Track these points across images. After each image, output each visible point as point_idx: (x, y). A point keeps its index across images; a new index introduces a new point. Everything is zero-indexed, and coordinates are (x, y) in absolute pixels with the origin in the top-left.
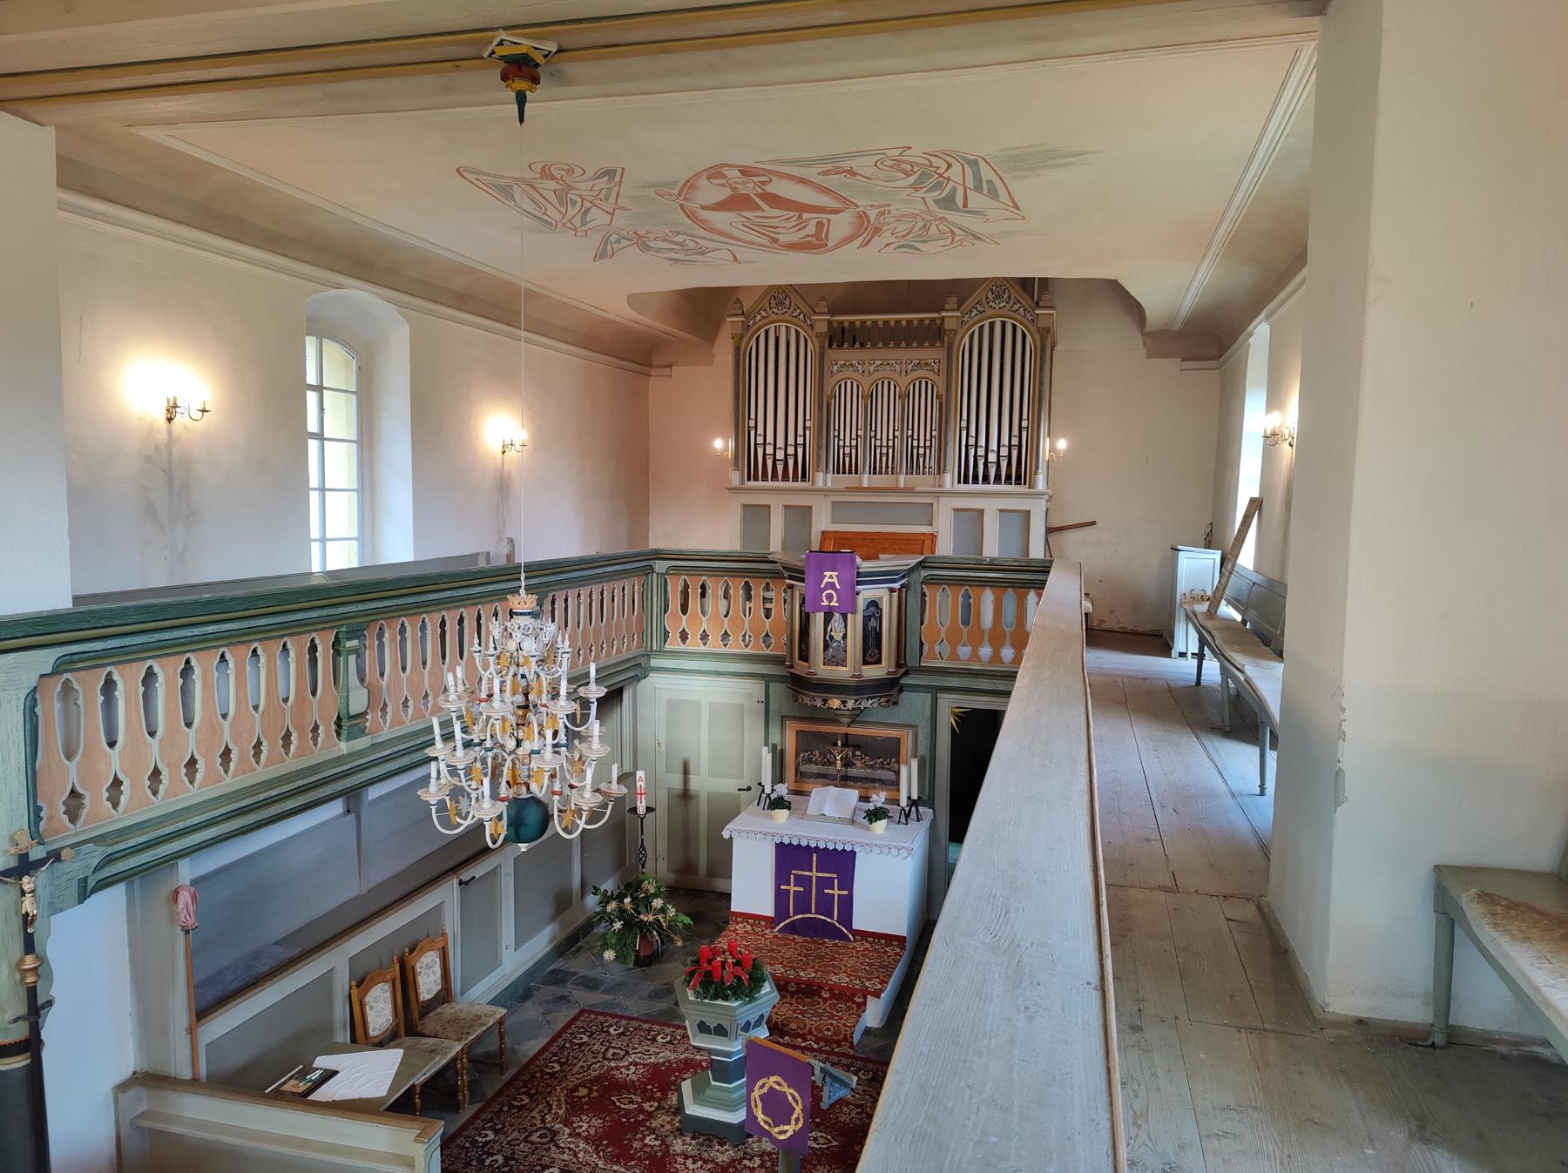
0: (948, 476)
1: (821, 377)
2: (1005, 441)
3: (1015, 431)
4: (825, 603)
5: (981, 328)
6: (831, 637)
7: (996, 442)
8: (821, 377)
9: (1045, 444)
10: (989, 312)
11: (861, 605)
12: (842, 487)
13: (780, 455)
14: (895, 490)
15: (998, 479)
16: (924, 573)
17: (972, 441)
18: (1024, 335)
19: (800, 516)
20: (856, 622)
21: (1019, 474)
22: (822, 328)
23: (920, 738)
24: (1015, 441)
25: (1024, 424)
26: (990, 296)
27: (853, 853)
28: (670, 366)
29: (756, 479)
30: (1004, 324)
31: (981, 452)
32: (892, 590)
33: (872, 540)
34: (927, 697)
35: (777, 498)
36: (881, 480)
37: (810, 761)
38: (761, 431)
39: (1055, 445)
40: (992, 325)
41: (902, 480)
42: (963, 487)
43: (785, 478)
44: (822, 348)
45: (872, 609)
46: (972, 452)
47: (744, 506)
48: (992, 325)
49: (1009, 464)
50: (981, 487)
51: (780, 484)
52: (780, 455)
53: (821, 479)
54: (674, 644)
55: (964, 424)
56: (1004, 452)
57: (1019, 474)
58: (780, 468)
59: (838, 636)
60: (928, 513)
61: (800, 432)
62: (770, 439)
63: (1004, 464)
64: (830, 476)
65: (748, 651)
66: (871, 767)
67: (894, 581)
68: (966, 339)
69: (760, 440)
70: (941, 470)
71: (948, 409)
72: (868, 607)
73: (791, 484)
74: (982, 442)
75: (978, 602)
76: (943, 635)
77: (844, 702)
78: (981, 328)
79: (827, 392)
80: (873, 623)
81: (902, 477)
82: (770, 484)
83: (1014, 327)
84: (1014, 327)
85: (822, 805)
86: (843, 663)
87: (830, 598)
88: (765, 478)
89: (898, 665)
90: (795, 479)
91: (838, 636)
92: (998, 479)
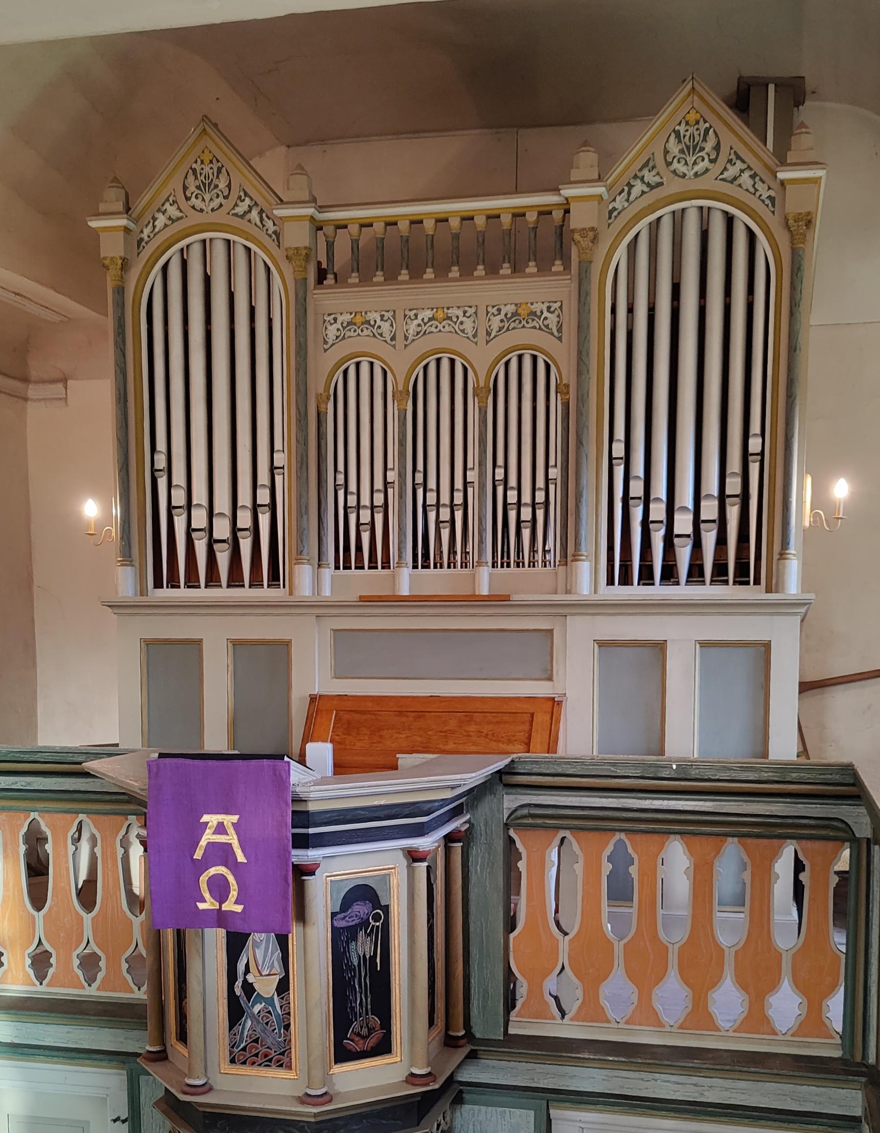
0: (584, 568)
1: (302, 351)
2: (711, 485)
7: (691, 492)
8: (302, 351)
10: (673, 187)
11: (322, 897)
12: (352, 596)
14: (472, 600)
16: (511, 801)
17: (636, 488)
19: (264, 661)
20: (314, 943)
21: (743, 561)
25: (755, 445)
26: (674, 147)
28: (64, 380)
29: (174, 583)
30: (704, 214)
32: (414, 856)
33: (420, 715)
35: (217, 624)
36: (436, 581)
38: (179, 477)
39: (822, 493)
40: (678, 218)
41: (485, 580)
42: (619, 592)
43: (235, 580)
45: (361, 909)
48: (678, 218)
50: (658, 591)
51: (223, 593)
53: (306, 580)
55: (619, 450)
56: (709, 510)
57: (743, 561)
60: (541, 652)
61: (263, 478)
62: (200, 495)
63: (709, 539)
64: (328, 573)
65: (92, 991)
67: (420, 831)
68: (621, 254)
69: (179, 497)
70: (568, 555)
71: (579, 413)
72: (347, 902)
73: (246, 593)
74: (660, 489)
75: (650, 873)
76: (563, 958)
80: (363, 946)
82: (203, 593)
83: (730, 220)
86: (280, 1058)
87: (219, 889)
88: (192, 581)
89: (450, 1042)
90: (255, 582)
92: (696, 572)
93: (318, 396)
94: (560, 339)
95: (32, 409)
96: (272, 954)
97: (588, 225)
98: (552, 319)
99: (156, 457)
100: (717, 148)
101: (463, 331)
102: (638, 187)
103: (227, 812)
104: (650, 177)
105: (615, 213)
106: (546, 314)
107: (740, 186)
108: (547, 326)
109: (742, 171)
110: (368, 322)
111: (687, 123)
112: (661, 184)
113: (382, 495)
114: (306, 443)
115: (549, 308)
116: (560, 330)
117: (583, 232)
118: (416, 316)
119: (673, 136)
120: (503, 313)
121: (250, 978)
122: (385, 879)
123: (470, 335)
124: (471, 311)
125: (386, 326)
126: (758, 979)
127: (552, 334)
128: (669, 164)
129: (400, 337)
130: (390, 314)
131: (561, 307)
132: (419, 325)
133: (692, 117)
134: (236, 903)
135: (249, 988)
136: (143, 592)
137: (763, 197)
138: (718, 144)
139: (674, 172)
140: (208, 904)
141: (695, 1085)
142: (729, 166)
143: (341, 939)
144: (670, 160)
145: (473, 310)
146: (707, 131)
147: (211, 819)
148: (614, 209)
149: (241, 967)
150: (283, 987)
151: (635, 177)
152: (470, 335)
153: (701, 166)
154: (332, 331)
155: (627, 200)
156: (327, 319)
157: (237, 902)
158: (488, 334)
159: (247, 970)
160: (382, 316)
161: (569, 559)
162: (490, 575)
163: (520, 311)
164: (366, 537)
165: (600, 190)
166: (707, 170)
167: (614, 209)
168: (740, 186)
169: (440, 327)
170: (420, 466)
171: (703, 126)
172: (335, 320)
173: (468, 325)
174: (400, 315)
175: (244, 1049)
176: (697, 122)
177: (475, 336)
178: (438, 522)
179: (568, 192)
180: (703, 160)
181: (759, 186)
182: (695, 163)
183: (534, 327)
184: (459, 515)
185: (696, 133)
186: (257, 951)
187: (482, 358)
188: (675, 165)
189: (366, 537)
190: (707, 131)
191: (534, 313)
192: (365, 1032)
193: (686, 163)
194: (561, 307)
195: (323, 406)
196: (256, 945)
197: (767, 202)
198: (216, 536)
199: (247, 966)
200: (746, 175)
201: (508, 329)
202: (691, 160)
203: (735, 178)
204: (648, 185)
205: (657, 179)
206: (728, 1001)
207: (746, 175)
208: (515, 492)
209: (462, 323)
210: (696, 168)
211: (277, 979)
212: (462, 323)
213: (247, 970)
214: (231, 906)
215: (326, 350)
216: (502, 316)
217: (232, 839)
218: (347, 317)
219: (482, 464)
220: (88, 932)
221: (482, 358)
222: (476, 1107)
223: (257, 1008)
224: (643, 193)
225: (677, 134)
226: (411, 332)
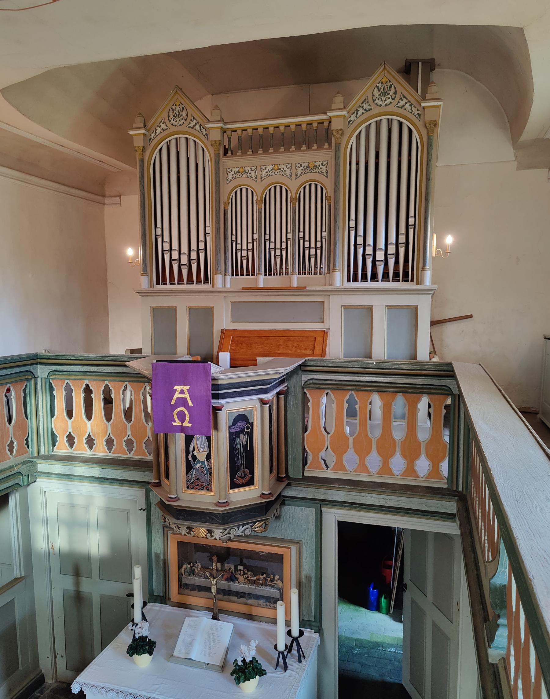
0: (337, 276)
1: (217, 183)
3: (402, 230)
5: (368, 128)
7: (383, 242)
8: (217, 183)
9: (432, 241)
11: (224, 420)
12: (239, 287)
13: (184, 260)
14: (290, 289)
16: (305, 377)
17: (360, 241)
18: (410, 131)
19: (202, 315)
22: (216, 136)
23: (304, 555)
24: (402, 239)
26: (376, 93)
28: (120, 196)
29: (164, 283)
30: (390, 122)
31: (369, 250)
32: (263, 402)
34: (310, 512)
36: (274, 281)
37: (192, 572)
38: (166, 238)
40: (378, 124)
41: (295, 280)
42: (353, 285)
43: (190, 281)
44: (217, 156)
45: (241, 424)
46: (360, 251)
47: (190, 308)
48: (378, 124)
49: (397, 262)
50: (370, 284)
53: (221, 281)
54: (62, 449)
55: (352, 224)
58: (185, 272)
60: (319, 310)
61: (202, 238)
62: (175, 245)
64: (229, 278)
65: (131, 456)
66: (254, 582)
67: (266, 391)
68: (353, 139)
69: (166, 247)
70: (331, 270)
71: (335, 209)
72: (235, 422)
76: (327, 443)
78: (368, 128)
79: (224, 198)
80: (242, 440)
81: (295, 277)
82: (176, 287)
83: (401, 124)
84: (401, 124)
85: (191, 644)
86: (208, 487)
87: (182, 416)
88: (172, 282)
90: (198, 282)
93: (224, 203)
94: (327, 177)
95: (107, 208)
96: (204, 443)
97: (339, 128)
98: (324, 168)
99: (157, 230)
100: (395, 93)
101: (286, 174)
102: (361, 111)
103: (185, 385)
104: (366, 106)
105: (351, 122)
106: (321, 166)
107: (405, 109)
108: (322, 172)
109: (406, 103)
110: (245, 171)
111: (382, 83)
112: (371, 109)
113: (251, 245)
114: (219, 223)
115: (322, 164)
116: (327, 173)
117: (337, 131)
118: (266, 168)
119: (376, 88)
120: (303, 166)
121: (195, 453)
122: (251, 412)
123: (289, 176)
124: (289, 166)
125: (253, 173)
126: (411, 455)
127: (324, 175)
128: (374, 101)
129: (259, 177)
130: (254, 168)
131: (327, 163)
132: (267, 172)
133: (384, 80)
134: (189, 423)
135: (194, 457)
136: (152, 286)
137: (415, 114)
138: (396, 91)
139: (377, 104)
140: (177, 423)
141: (384, 499)
142: (400, 101)
143: (233, 437)
144: (374, 99)
145: (290, 165)
146: (391, 86)
147: (178, 388)
148: (351, 121)
149: (191, 448)
150: (209, 457)
151: (360, 107)
152: (289, 176)
153: (388, 101)
154: (230, 175)
155: (356, 117)
156: (228, 170)
157: (189, 423)
158: (296, 175)
159: (194, 450)
160: (251, 169)
161: (331, 271)
162: (297, 278)
163: (310, 165)
164: (245, 262)
165: (344, 113)
166: (391, 103)
167: (351, 121)
168: (405, 109)
169: (276, 173)
170: (268, 232)
171: (389, 84)
172: (232, 170)
173: (288, 172)
174: (259, 168)
175: (192, 483)
176: (387, 82)
177: (291, 176)
178: (275, 256)
179: (330, 114)
180: (389, 98)
181: (414, 109)
182: (386, 100)
183: (316, 172)
184: (284, 253)
185: (386, 87)
186: (198, 442)
187: (294, 185)
188: (377, 101)
189: (245, 262)
190: (391, 86)
191: (316, 166)
192: (243, 476)
193: (382, 100)
194: (327, 163)
195: (226, 207)
196: (197, 439)
197: (417, 116)
198: (182, 262)
199: (194, 448)
200: (408, 104)
201: (305, 173)
202: (384, 98)
203: (403, 106)
204: (365, 110)
205: (369, 107)
206: (398, 463)
207: (408, 104)
208: (308, 243)
209: (285, 171)
210: (386, 102)
211: (206, 453)
212: (285, 171)
213: (194, 450)
214: (186, 424)
215: (227, 184)
216: (302, 168)
217: (187, 396)
218: (237, 169)
219: (294, 231)
220: (129, 431)
221: (294, 185)
222: (290, 507)
223: (198, 466)
224: (363, 113)
225: (378, 87)
226: (264, 175)
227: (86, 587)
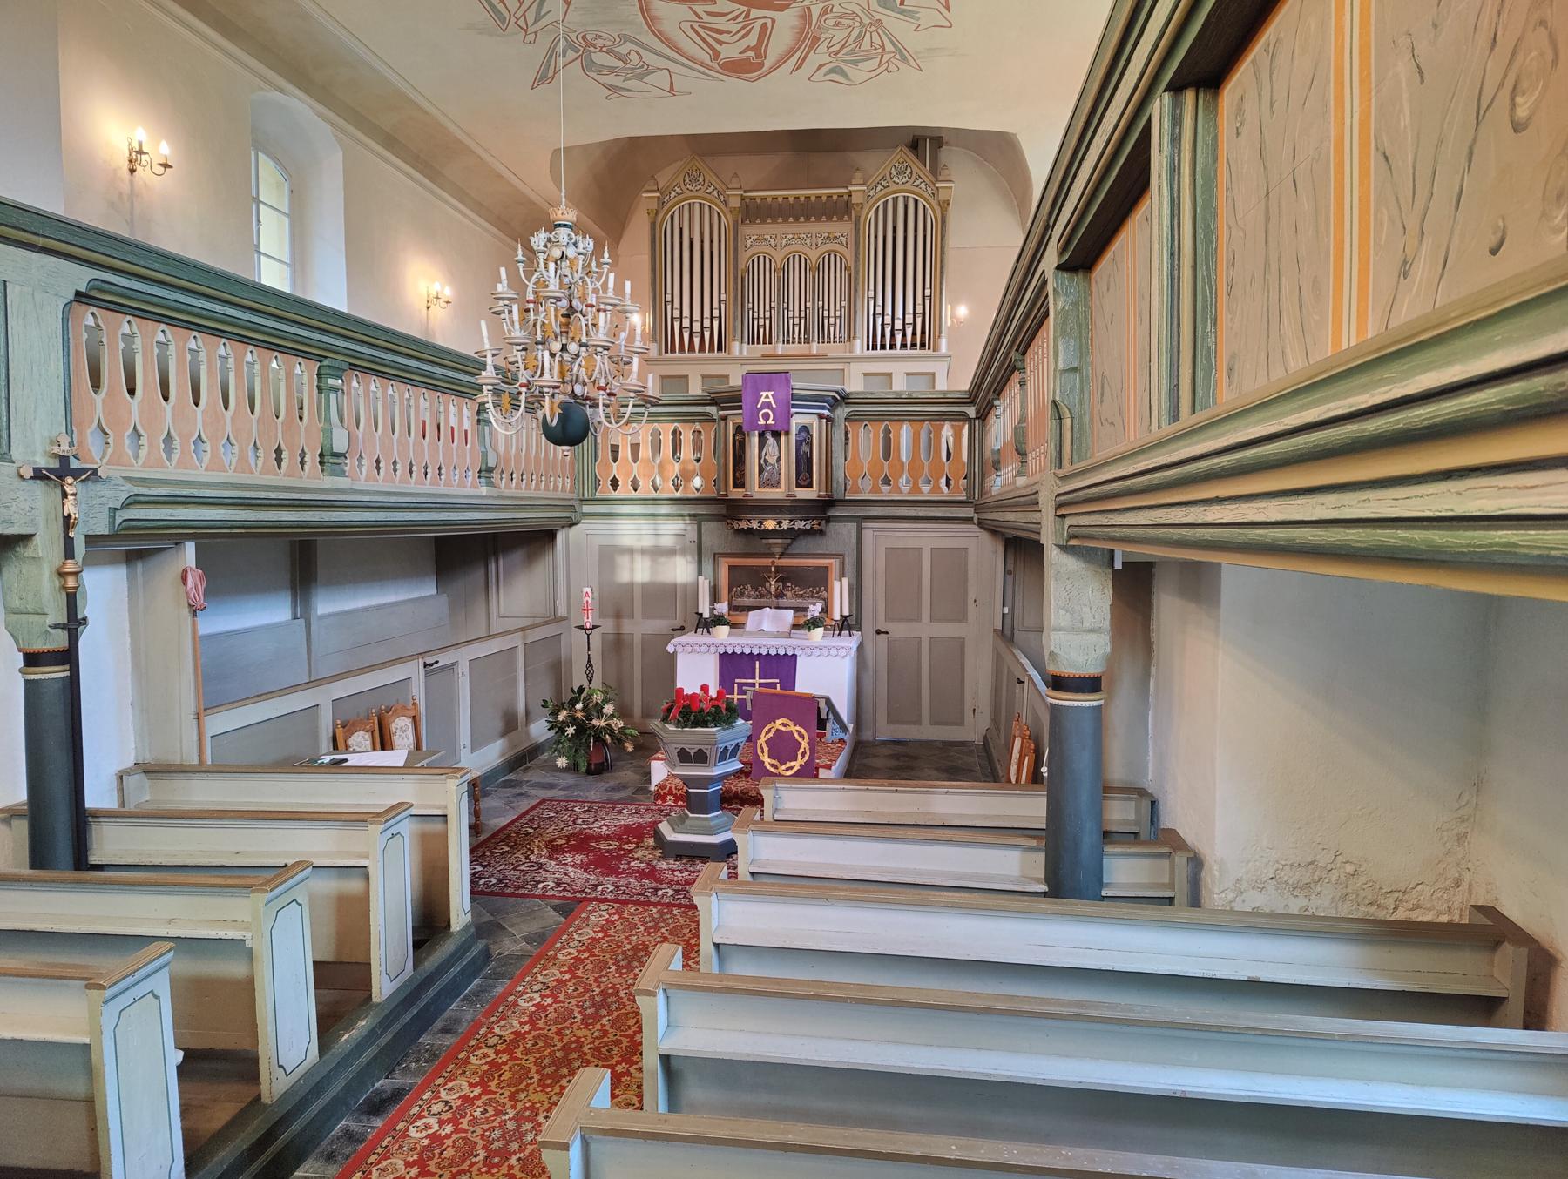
0: (858, 342)
2: (910, 309)
4: (762, 422)
5: (886, 203)
6: (766, 461)
10: (894, 187)
15: (904, 346)
24: (919, 309)
25: (927, 292)
27: (794, 656)
31: (888, 319)
34: (853, 526)
52: (697, 327)
55: (872, 294)
56: (909, 319)
59: (772, 460)
65: (678, 495)
77: (779, 523)
79: (742, 266)
80: (804, 448)
84: (916, 201)
86: (778, 485)
87: (766, 417)
91: (772, 460)
187: (814, 255)
221: (814, 255)
227: (627, 627)
